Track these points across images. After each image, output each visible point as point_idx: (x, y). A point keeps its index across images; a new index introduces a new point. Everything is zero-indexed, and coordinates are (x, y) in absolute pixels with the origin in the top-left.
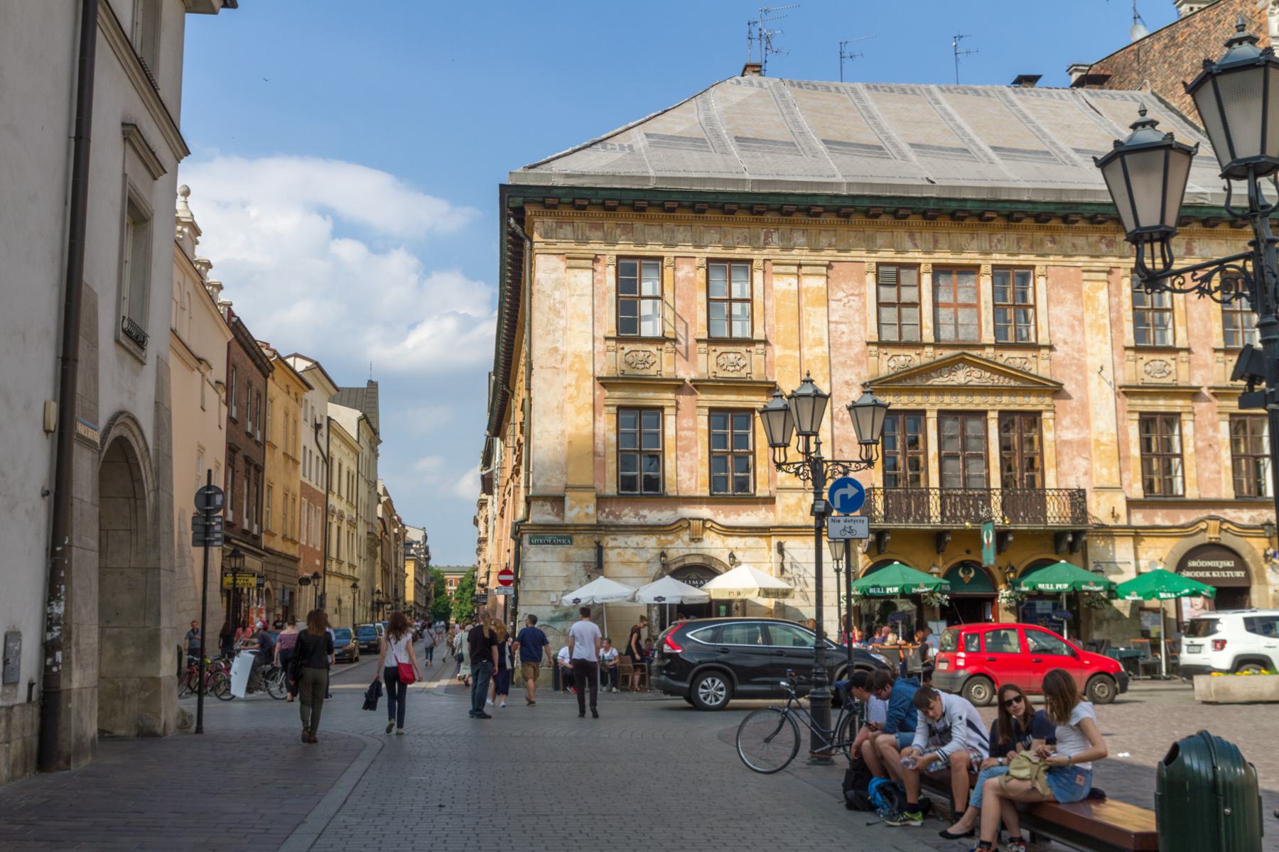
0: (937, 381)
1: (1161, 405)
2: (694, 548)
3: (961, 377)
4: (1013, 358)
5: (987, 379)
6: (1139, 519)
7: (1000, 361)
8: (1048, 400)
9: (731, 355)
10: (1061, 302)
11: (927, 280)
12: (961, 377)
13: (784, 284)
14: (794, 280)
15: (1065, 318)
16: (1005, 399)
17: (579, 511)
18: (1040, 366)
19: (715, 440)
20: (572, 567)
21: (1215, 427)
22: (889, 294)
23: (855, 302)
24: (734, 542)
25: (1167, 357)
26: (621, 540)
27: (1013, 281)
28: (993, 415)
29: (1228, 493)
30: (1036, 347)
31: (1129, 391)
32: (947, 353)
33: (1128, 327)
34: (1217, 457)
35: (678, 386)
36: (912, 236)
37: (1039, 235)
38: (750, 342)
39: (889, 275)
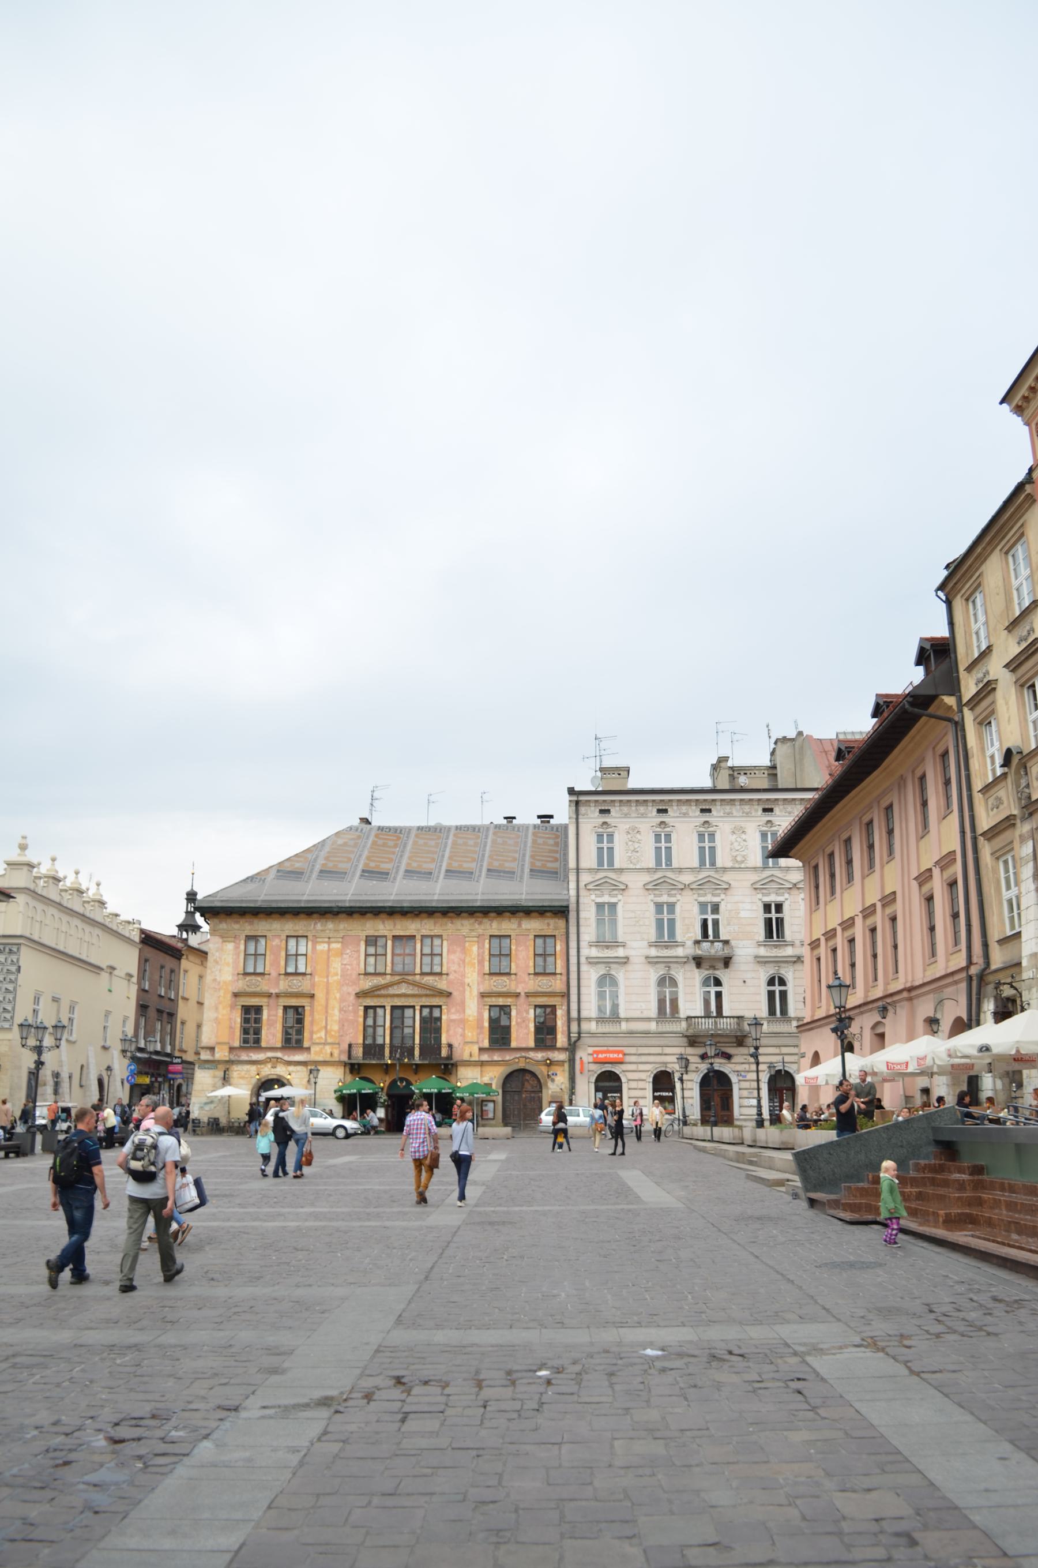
0: (383, 992)
1: (501, 1001)
3: (403, 989)
4: (429, 980)
6: (485, 1057)
7: (423, 982)
9: (295, 981)
10: (454, 952)
11: (389, 943)
12: (403, 989)
13: (322, 947)
14: (326, 945)
16: (424, 999)
17: (221, 1054)
18: (442, 984)
20: (217, 1080)
21: (528, 1012)
22: (371, 950)
23: (355, 955)
24: (291, 1068)
25: (505, 978)
26: (240, 1067)
29: (532, 1044)
30: (440, 974)
31: (483, 995)
32: (397, 978)
33: (487, 964)
34: (527, 1027)
35: (269, 995)
36: (383, 922)
37: (445, 920)
38: (304, 974)
39: (371, 941)
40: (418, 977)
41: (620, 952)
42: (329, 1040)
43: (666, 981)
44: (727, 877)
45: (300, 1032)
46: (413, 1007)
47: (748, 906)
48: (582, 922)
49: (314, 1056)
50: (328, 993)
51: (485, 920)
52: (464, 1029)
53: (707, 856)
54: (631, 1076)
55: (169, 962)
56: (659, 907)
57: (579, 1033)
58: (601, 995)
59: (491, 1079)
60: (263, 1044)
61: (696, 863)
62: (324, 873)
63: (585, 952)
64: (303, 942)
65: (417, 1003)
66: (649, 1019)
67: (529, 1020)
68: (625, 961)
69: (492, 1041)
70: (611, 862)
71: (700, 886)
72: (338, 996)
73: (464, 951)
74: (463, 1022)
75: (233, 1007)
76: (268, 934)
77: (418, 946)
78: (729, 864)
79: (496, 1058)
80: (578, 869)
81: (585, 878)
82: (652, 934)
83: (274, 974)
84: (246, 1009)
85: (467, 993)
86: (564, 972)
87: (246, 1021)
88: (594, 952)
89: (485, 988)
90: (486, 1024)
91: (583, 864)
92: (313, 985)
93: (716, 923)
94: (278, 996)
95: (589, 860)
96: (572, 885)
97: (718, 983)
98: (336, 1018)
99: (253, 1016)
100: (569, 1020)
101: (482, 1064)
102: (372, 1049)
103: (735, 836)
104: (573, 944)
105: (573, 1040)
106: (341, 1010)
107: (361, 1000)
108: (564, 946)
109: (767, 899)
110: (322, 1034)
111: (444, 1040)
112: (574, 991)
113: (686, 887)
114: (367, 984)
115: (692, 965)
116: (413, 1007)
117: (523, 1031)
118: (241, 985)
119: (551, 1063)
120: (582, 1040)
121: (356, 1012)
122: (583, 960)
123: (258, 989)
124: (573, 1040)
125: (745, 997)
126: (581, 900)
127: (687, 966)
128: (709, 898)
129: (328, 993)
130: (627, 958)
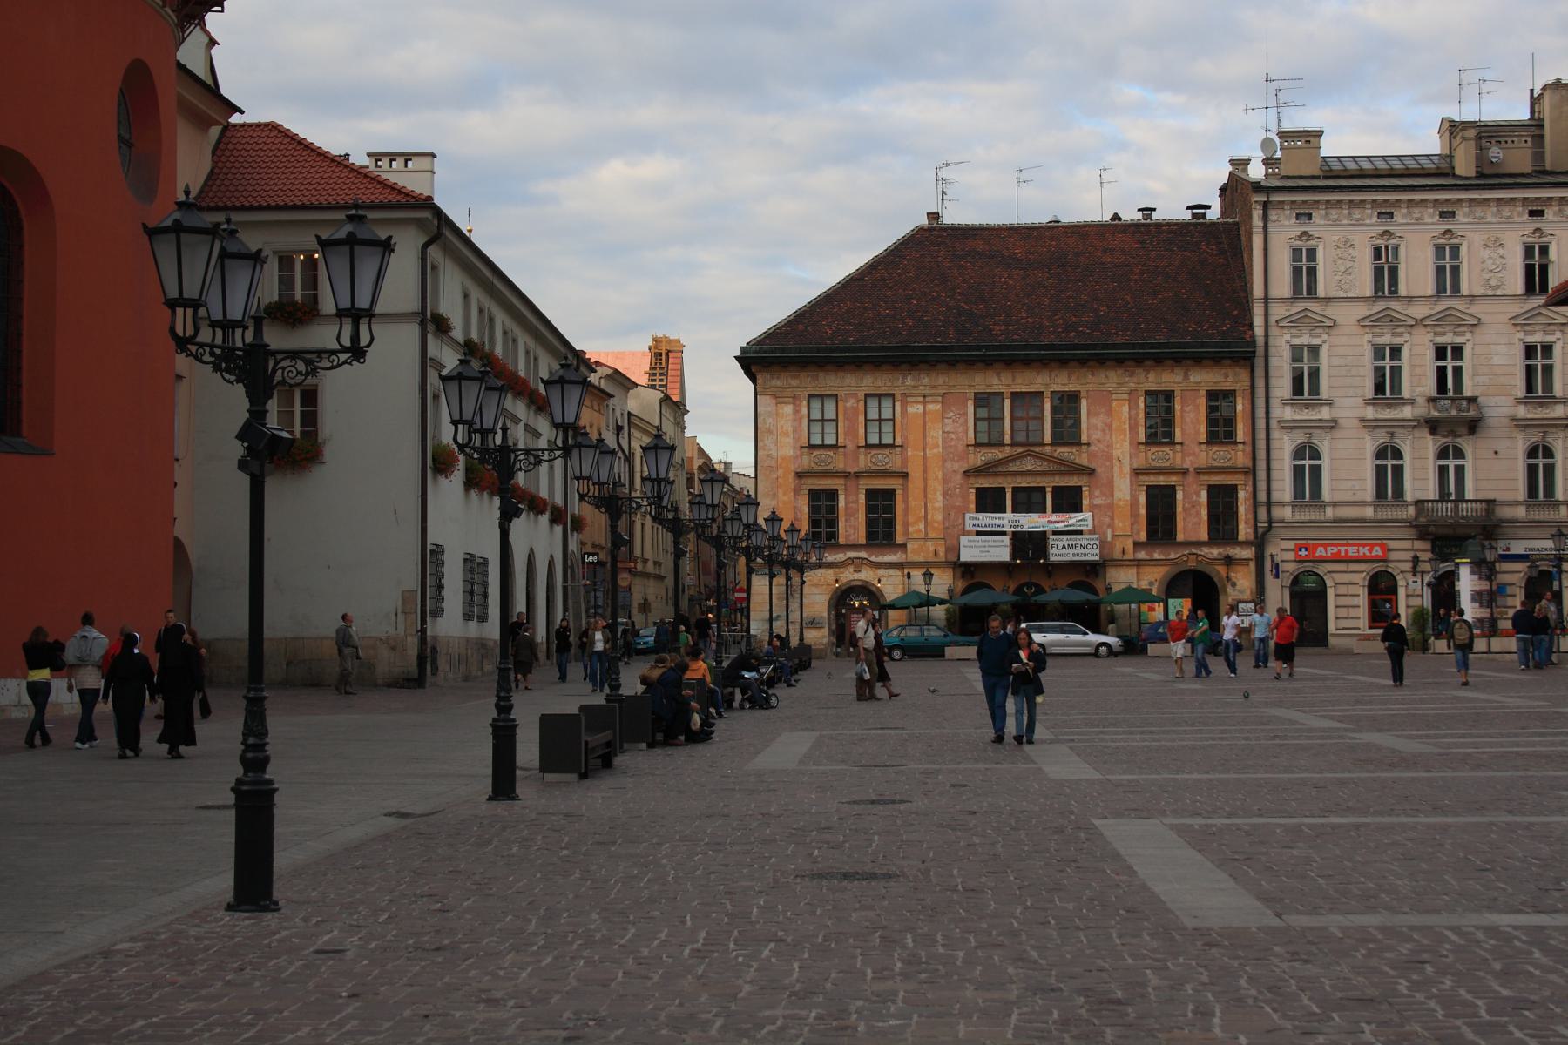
1: (1161, 480)
2: (857, 576)
3: (1029, 465)
5: (1045, 466)
6: (1142, 555)
8: (1085, 479)
9: (881, 455)
10: (1097, 414)
11: (1007, 403)
12: (1029, 465)
13: (915, 409)
15: (1100, 425)
16: (1057, 478)
18: (1082, 459)
19: (870, 509)
21: (1198, 495)
22: (983, 413)
24: (881, 572)
27: (1068, 403)
28: (1049, 490)
29: (1204, 536)
30: (1079, 444)
31: (1137, 472)
34: (1198, 514)
35: (846, 475)
36: (998, 375)
38: (892, 446)
39: (982, 400)
40: (1048, 449)
41: (1325, 413)
42: (931, 535)
43: (1388, 451)
44: (1476, 309)
45: (891, 523)
46: (1042, 490)
47: (1503, 349)
48: (1272, 372)
50: (925, 471)
51: (1139, 371)
52: (1112, 519)
53: (1447, 278)
54: (1339, 578)
56: (1378, 352)
57: (1270, 521)
58: (1298, 472)
59: (1151, 583)
60: (842, 541)
61: (1430, 289)
63: (1276, 413)
64: (886, 403)
65: (1049, 483)
66: (1364, 503)
67: (1200, 505)
68: (1333, 425)
69: (1151, 533)
70: (1312, 289)
71: (1439, 321)
72: (940, 475)
73: (1109, 412)
74: (1111, 507)
75: (797, 491)
76: (841, 392)
77: (1047, 406)
78: (1478, 291)
79: (1156, 556)
80: (1266, 299)
81: (1278, 311)
82: (1369, 392)
83: (850, 446)
84: (815, 495)
85: (1116, 469)
86: (1248, 439)
87: (814, 509)
88: (1288, 414)
89: (1140, 462)
90: (1143, 511)
91: (1273, 293)
92: (905, 461)
93: (1458, 371)
94: (858, 475)
95: (1282, 285)
96: (1258, 321)
97: (1459, 454)
98: (939, 504)
99: (824, 504)
100: (1255, 504)
101: (1138, 563)
103: (1488, 251)
104: (1260, 402)
105: (1260, 531)
106: (944, 494)
107: (972, 480)
108: (1249, 406)
109: (1530, 339)
110: (922, 526)
112: (1261, 465)
113: (1419, 322)
115: (1425, 432)
116: (1042, 490)
117: (1192, 519)
118: (805, 462)
119: (1229, 561)
120: (1273, 531)
121: (965, 497)
122: (1274, 424)
123: (830, 468)
124: (1260, 531)
125: (1495, 473)
126: (1271, 342)
127: (1417, 433)
128: (1448, 339)
129: (925, 471)
130: (1335, 421)
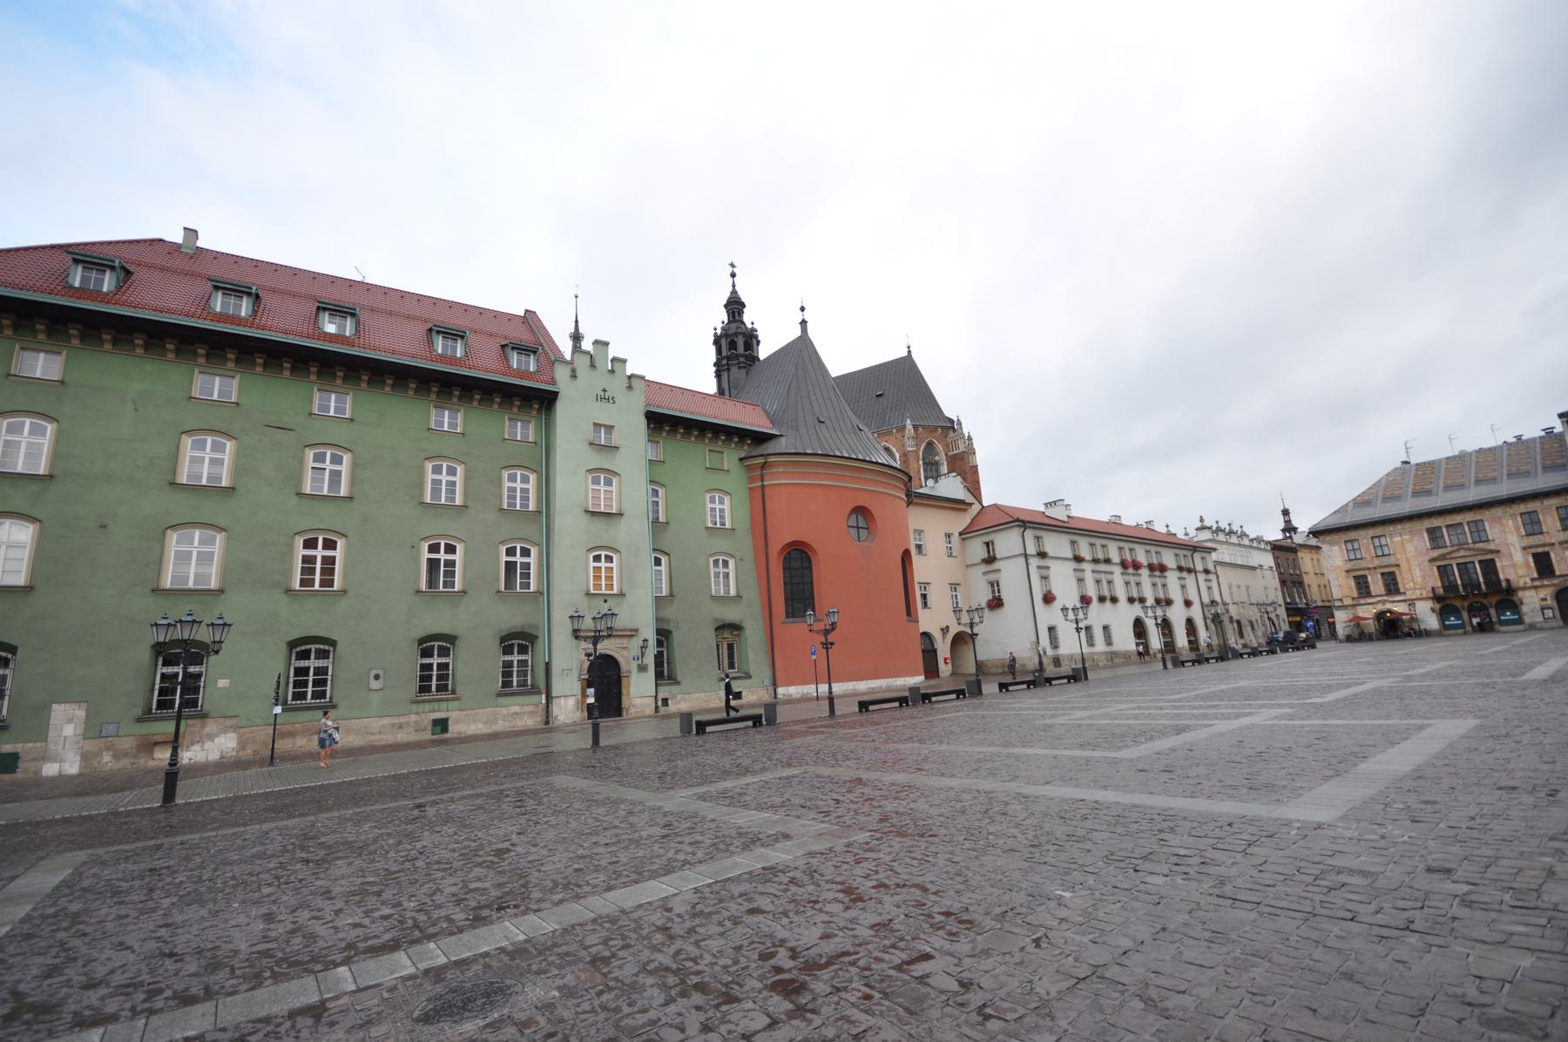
1: (1540, 550)
3: (1462, 553)
12: (1462, 553)
17: (1348, 602)
18: (1491, 546)
27: (1477, 526)
31: (1524, 548)
45: (1396, 584)
49: (1409, 595)
55: (1291, 556)
62: (1385, 499)
74: (1514, 565)
101: (1536, 587)
102: (1450, 587)
111: (1502, 577)
114: (1436, 553)
118: (1349, 566)
